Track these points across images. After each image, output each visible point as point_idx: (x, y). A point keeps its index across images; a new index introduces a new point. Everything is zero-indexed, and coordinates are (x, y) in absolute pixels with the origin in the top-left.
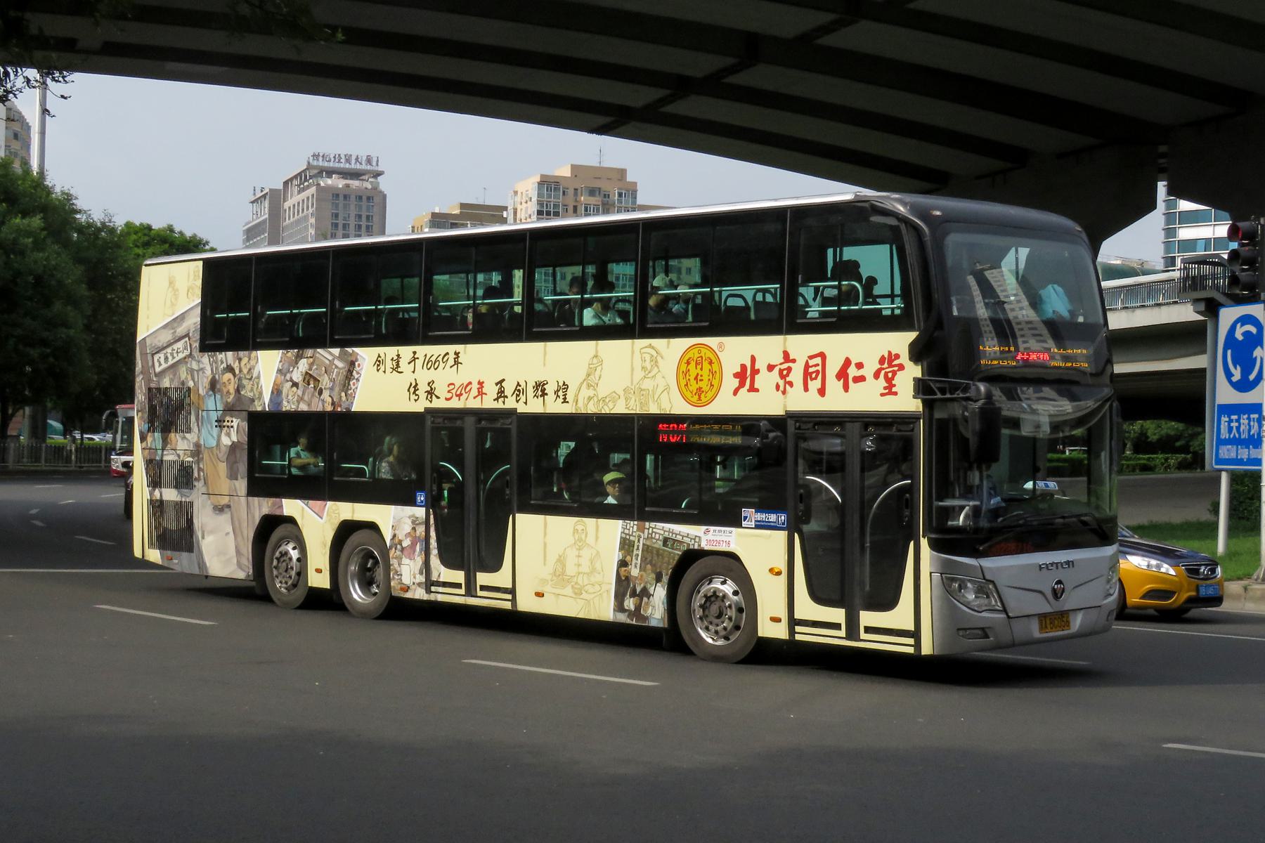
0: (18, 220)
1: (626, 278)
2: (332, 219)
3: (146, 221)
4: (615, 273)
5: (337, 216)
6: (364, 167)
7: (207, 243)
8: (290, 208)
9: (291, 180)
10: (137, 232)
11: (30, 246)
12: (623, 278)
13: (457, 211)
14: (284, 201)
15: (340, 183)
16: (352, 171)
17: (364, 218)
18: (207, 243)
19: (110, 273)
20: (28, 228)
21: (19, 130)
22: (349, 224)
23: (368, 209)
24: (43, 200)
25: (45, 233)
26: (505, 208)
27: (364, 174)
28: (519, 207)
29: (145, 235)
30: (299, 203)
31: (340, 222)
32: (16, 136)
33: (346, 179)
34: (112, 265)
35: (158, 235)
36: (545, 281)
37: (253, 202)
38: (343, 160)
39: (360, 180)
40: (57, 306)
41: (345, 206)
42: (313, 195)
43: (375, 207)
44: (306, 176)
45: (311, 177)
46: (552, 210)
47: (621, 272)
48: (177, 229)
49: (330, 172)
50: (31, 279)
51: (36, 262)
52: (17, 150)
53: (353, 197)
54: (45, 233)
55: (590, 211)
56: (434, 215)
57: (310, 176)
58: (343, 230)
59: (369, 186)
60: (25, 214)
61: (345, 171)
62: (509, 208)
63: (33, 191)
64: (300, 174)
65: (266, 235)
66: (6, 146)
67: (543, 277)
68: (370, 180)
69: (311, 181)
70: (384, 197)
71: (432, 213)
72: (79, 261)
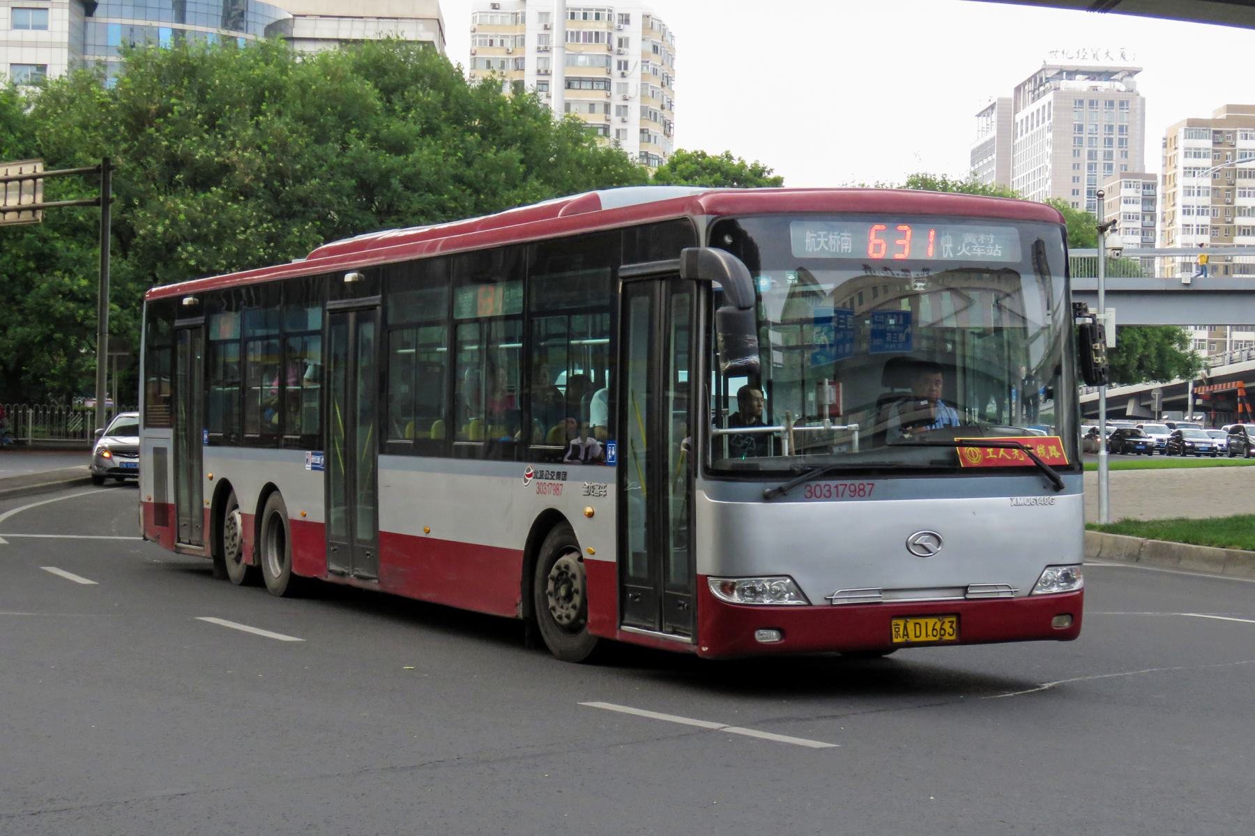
0: (490, 155)
3: (699, 148)
5: (1080, 128)
6: (1117, 63)
8: (1022, 120)
9: (1024, 84)
10: (687, 160)
13: (1223, 116)
14: (1016, 112)
15: (1081, 84)
16: (1100, 70)
17: (1116, 130)
20: (501, 163)
21: (660, 42)
24: (526, 128)
25: (522, 166)
27: (1116, 73)
29: (698, 163)
30: (1033, 114)
32: (655, 49)
33: (1094, 79)
35: (711, 163)
37: (979, 115)
38: (1090, 56)
39: (1112, 80)
42: (1050, 103)
44: (1041, 80)
45: (1048, 80)
48: (735, 156)
49: (1072, 74)
52: (656, 65)
53: (1101, 104)
57: (1047, 78)
59: (1123, 88)
60: (506, 144)
61: (1094, 70)
63: (515, 118)
64: (1034, 76)
65: (994, 156)
66: (642, 62)
68: (1125, 80)
69: (1048, 85)
70: (1143, 100)
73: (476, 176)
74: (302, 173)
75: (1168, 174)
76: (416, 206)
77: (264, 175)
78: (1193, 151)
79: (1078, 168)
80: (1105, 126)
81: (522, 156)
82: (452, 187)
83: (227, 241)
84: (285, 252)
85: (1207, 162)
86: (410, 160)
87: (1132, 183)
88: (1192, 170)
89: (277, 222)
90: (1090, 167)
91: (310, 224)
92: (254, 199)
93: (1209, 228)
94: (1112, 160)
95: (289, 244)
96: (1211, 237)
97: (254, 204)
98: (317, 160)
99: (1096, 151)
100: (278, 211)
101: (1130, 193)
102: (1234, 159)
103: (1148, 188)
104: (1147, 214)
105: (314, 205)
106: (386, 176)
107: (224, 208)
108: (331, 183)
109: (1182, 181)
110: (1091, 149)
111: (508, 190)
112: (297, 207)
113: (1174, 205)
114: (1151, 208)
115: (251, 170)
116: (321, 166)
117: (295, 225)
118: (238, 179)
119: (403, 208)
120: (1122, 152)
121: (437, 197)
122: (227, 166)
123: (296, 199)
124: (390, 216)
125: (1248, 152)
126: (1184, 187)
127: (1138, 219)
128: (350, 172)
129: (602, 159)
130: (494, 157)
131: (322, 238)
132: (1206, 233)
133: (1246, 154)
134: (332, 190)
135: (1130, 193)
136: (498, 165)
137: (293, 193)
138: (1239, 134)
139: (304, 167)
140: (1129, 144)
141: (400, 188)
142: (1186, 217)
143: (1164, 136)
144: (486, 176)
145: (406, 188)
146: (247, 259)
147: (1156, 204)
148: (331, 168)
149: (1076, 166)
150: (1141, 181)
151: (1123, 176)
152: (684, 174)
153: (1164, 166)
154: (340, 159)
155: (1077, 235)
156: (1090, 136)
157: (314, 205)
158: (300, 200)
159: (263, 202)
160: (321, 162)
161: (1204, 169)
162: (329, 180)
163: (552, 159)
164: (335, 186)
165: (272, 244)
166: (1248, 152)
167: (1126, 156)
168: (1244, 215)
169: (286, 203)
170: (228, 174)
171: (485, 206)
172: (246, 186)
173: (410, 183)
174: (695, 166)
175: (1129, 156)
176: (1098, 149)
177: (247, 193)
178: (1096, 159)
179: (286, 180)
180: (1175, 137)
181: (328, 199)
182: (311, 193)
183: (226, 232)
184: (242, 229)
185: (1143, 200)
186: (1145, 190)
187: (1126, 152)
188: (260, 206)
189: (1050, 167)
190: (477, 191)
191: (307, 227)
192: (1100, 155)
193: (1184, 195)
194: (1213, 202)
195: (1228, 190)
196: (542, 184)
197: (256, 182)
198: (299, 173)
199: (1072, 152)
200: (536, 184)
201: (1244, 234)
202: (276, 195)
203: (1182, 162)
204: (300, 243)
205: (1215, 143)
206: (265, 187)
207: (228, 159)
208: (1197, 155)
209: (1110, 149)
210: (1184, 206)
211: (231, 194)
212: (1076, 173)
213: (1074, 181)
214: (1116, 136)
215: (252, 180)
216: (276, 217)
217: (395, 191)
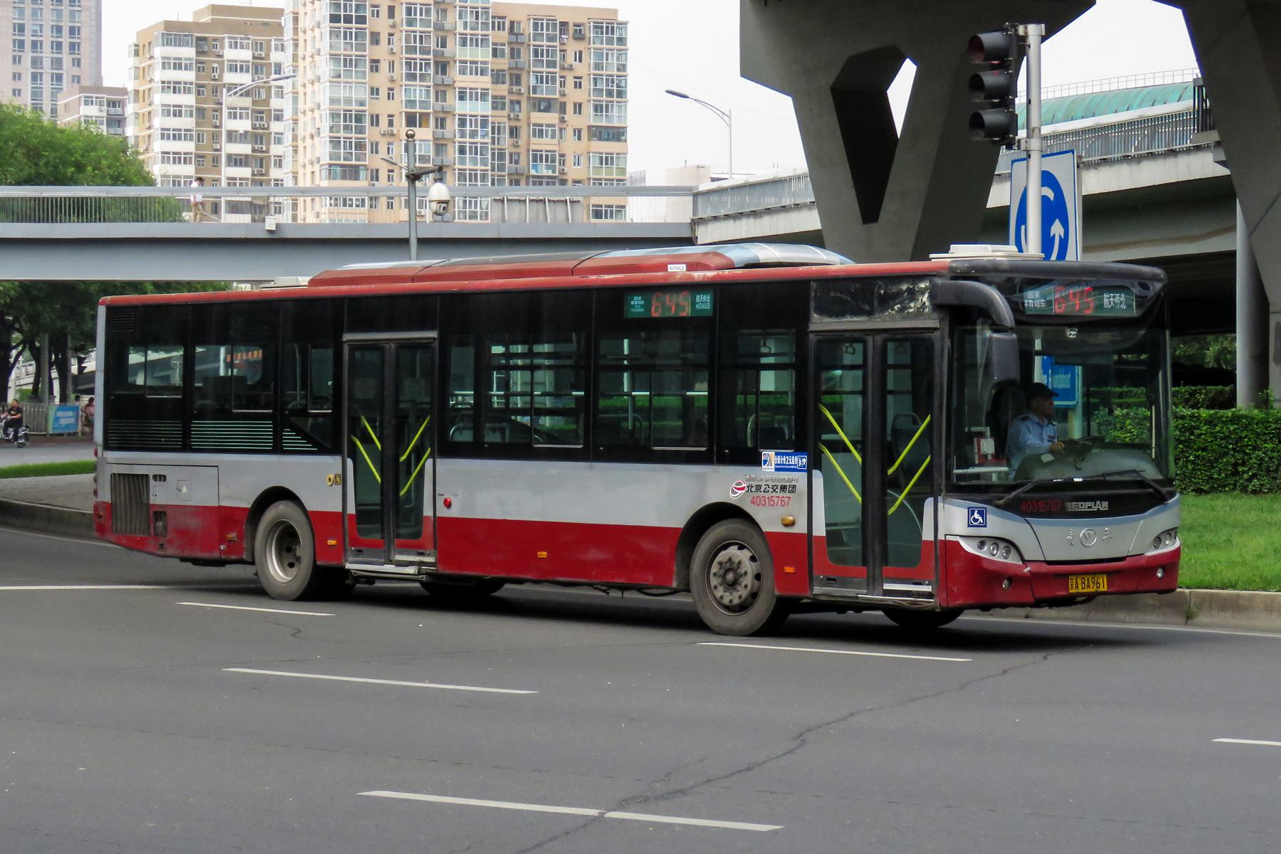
1: (476, 120)
2: (14, 35)
4: (458, 111)
5: (21, 28)
12: (471, 120)
13: (206, 19)
17: (66, 32)
22: (41, 42)
23: (72, 14)
26: (280, 12)
28: (301, 10)
31: (28, 39)
36: (346, 128)
41: (34, 13)
43: (83, 13)
46: (353, 14)
47: (468, 112)
55: (415, 15)
56: (169, 25)
58: (33, 52)
62: (285, 12)
67: (342, 123)
71: (166, 22)
75: (141, 89)
78: (172, 61)
79: (19, 79)
80: (52, 26)
85: (189, 76)
87: (94, 99)
88: (172, 85)
90: (35, 77)
93: (193, 156)
94: (61, 69)
96: (196, 169)
99: (41, 58)
101: (92, 111)
102: (222, 71)
103: (114, 106)
109: (159, 98)
110: (34, 54)
113: (149, 128)
114: (119, 131)
120: (73, 60)
125: (239, 64)
126: (163, 105)
132: (190, 163)
133: (236, 66)
135: (92, 111)
138: (227, 41)
140: (82, 49)
142: (165, 142)
143: (135, 41)
147: (124, 126)
149: (17, 77)
150: (105, 96)
153: (136, 78)
156: (35, 38)
161: (186, 83)
166: (239, 64)
167: (79, 65)
168: (236, 142)
175: (82, 65)
176: (44, 55)
178: (42, 68)
180: (150, 43)
186: (112, 110)
187: (79, 60)
192: (47, 64)
193: (163, 115)
194: (198, 124)
195: (215, 110)
199: (11, 58)
201: (236, 165)
203: (159, 75)
205: (199, 53)
208: (177, 66)
209: (60, 56)
210: (162, 129)
212: (18, 85)
213: (14, 94)
214: (66, 40)
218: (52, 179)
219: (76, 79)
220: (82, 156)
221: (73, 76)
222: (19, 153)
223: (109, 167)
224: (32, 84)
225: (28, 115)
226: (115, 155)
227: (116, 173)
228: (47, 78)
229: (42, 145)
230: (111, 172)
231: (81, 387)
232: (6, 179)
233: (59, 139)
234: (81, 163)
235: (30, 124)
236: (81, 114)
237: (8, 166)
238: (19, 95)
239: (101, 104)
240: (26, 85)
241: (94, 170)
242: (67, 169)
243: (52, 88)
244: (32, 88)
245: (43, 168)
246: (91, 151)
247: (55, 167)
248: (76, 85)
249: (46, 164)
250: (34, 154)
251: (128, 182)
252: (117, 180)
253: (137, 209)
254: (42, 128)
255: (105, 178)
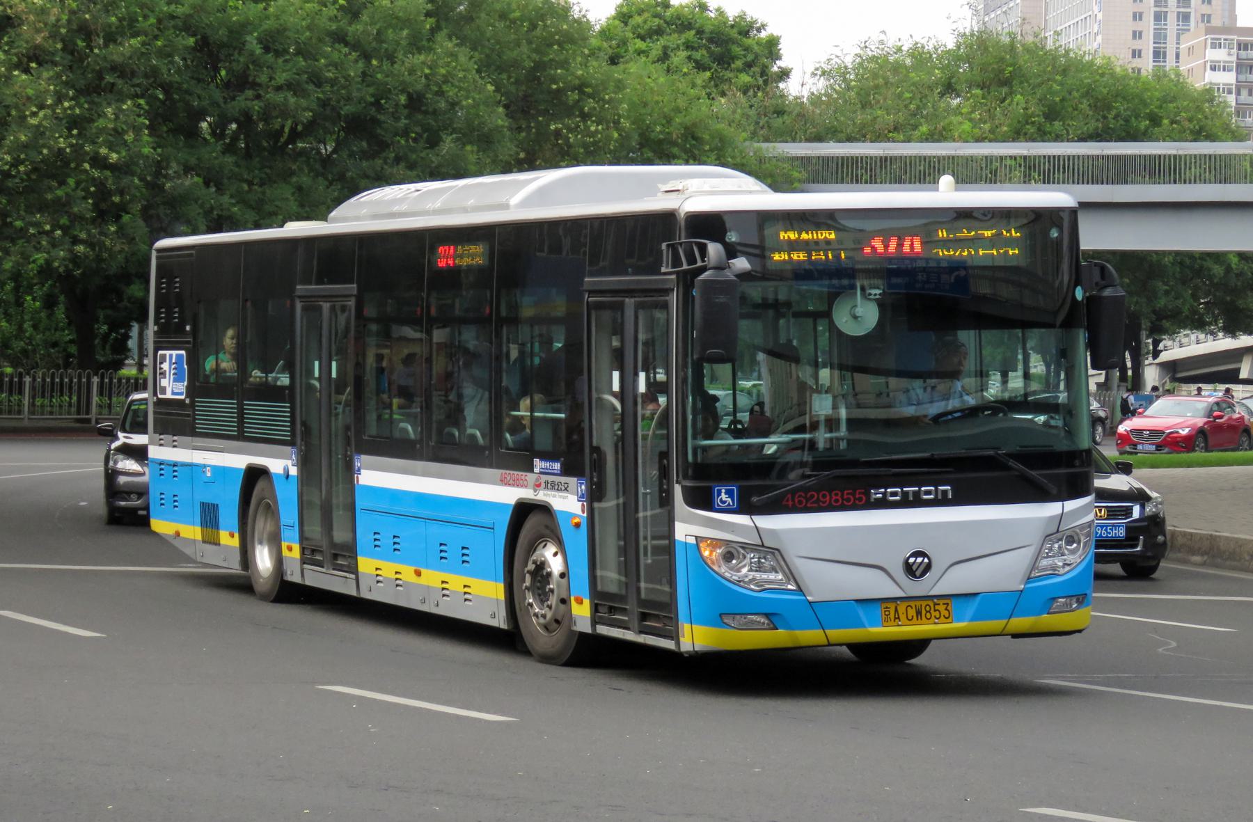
7: (763, 26)
10: (643, 11)
11: (404, 43)
18: (763, 26)
19: (554, 87)
20: (401, 14)
25: (431, 21)
29: (657, 16)
34: (559, 71)
40: (448, 144)
50: (403, 99)
51: (412, 72)
54: (429, 23)
72: (491, 64)
73: (364, 31)
74: (117, 28)
76: (281, 77)
77: (63, 31)
79: (1141, 19)
81: (429, 6)
82: (330, 49)
83: (14, 127)
84: (94, 143)
86: (271, 10)
89: (82, 100)
90: (1158, 17)
91: (129, 102)
92: (48, 66)
94: (1189, 7)
95: (101, 131)
97: (51, 73)
98: (141, 9)
100: (81, 83)
101: (1220, 55)
103: (1246, 48)
104: (1245, 87)
105: (133, 74)
106: (238, 32)
107: (8, 78)
108: (159, 43)
111: (413, 54)
112: (109, 78)
115: (46, 24)
116: (146, 17)
117: (109, 104)
118: (26, 36)
119: (263, 79)
121: (309, 62)
122: (9, 18)
123: (109, 66)
124: (242, 91)
127: (1230, 92)
128: (187, 27)
129: (537, 10)
130: (389, 5)
131: (147, 122)
134: (161, 53)
135: (1220, 55)
136: (397, 18)
137: (105, 59)
139: (120, 20)
141: (258, 51)
144: (379, 33)
145: (267, 49)
146: (41, 153)
148: (160, 21)
150: (1236, 37)
151: (1209, 31)
152: (642, 32)
154: (173, 7)
155: (1200, 120)
157: (133, 74)
158: (114, 68)
159: (62, 71)
160: (146, 11)
162: (156, 38)
163: (462, 8)
164: (165, 46)
165: (75, 132)
169: (93, 71)
170: (12, 32)
171: (379, 76)
172: (36, 47)
173: (273, 43)
174: (657, 21)
177: (35, 58)
178: (1166, 6)
179: (93, 37)
181: (154, 65)
182: (130, 58)
183: (9, 115)
184: (34, 109)
185: (1238, 66)
186: (1242, 53)
188: (58, 76)
189: (1100, 16)
190: (367, 57)
191: (125, 107)
196: (457, 45)
197: (50, 41)
198: (113, 29)
200: (450, 45)
202: (75, 58)
204: (115, 130)
206: (63, 50)
207: (11, 7)
211: (15, 59)
213: (1134, 36)
215: (44, 39)
216: (80, 92)
217: (252, 54)
218: (1124, 134)
219: (1206, 18)
220: (1161, 107)
221: (1203, 15)
222: (1084, 105)
223: (1190, 120)
224: (1155, 25)
225: (1098, 61)
226: (1198, 107)
227: (1197, 127)
228: (1172, 20)
229: (1112, 96)
230: (1192, 127)
231: (1179, 375)
232: (1068, 134)
233: (1133, 88)
234: (1157, 115)
235: (1100, 71)
236: (1207, 59)
237: (1072, 119)
238: (1140, 37)
239: (1231, 46)
240: (1148, 25)
241: (1172, 122)
242: (1140, 122)
243: (1178, 30)
244: (1155, 29)
245: (1113, 121)
246: (1170, 102)
247: (1127, 121)
248: (1202, 26)
249: (1116, 117)
250: (1101, 105)
251: (1211, 138)
252: (1200, 134)
253: (1220, 169)
254: (1113, 75)
255: (1184, 132)
